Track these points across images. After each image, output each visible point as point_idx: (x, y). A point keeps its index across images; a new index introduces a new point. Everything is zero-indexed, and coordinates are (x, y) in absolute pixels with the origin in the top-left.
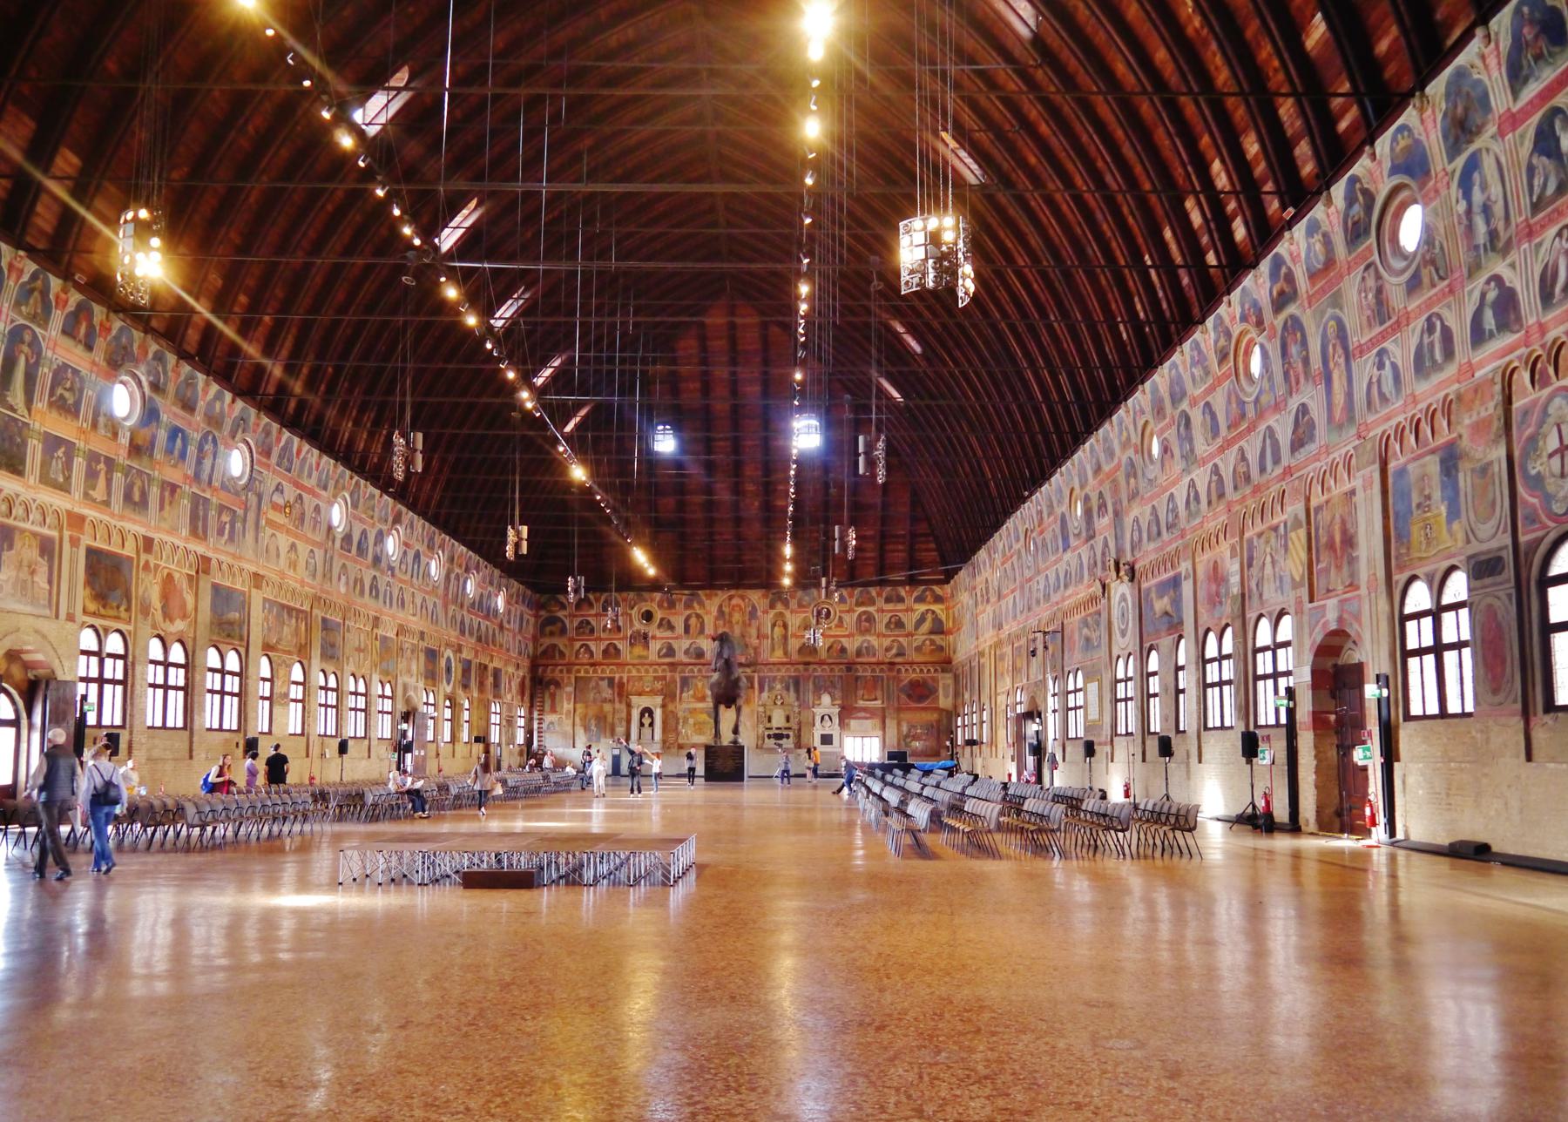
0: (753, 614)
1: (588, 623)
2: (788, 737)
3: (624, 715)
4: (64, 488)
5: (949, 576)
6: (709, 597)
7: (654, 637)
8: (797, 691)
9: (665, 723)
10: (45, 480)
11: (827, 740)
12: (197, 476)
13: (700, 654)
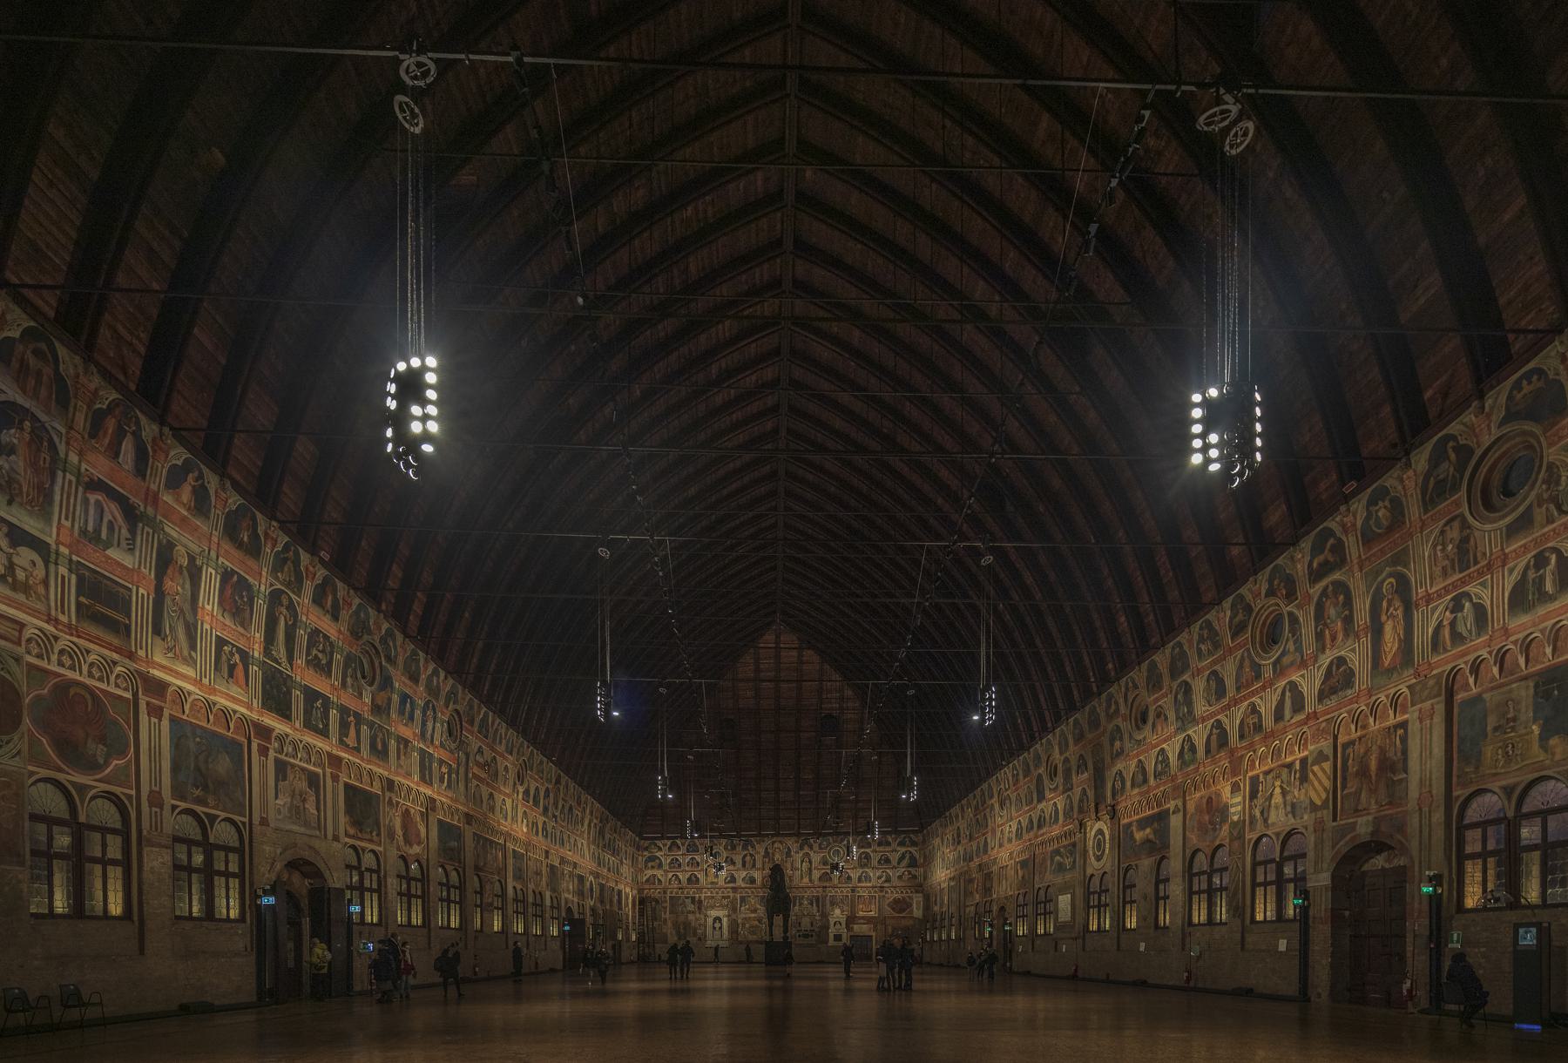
0: (788, 854)
4: (324, 733)
5: (922, 827)
10: (308, 725)
12: (423, 735)
13: (753, 881)
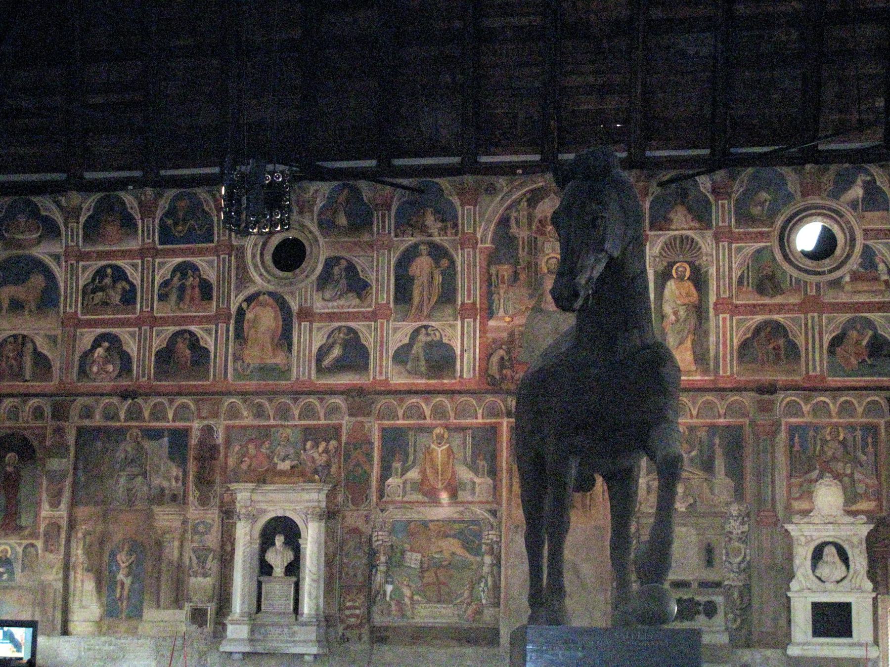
1: (119, 274)
2: (710, 610)
3: (212, 540)
6: (470, 197)
7: (306, 314)
8: (736, 472)
9: (332, 563)
11: (833, 620)
13: (441, 360)
